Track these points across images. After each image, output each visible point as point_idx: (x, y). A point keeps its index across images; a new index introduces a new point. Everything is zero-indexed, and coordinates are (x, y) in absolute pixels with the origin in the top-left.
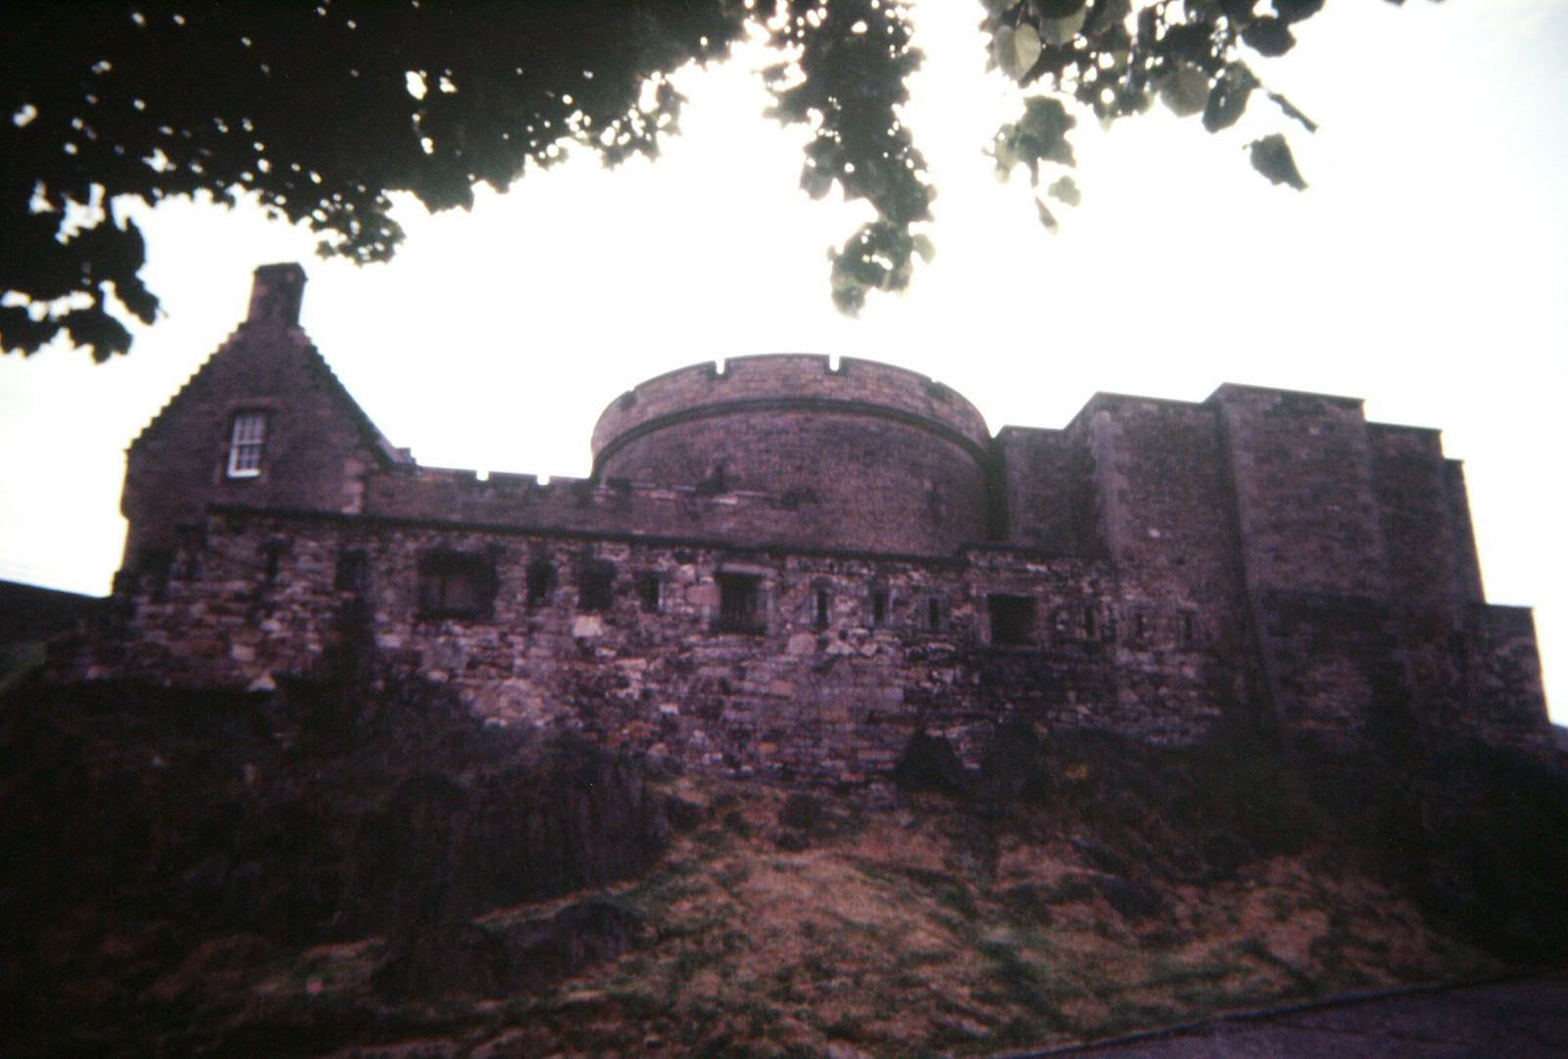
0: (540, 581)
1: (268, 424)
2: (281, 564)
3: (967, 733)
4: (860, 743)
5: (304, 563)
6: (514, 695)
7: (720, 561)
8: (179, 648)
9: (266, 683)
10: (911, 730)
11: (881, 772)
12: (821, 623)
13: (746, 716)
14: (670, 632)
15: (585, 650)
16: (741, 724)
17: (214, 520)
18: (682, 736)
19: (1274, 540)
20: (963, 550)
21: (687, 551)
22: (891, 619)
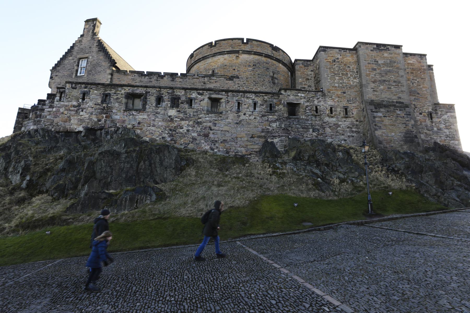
0: (159, 100)
1: (87, 61)
2: (86, 97)
3: (280, 140)
5: (92, 96)
6: (151, 131)
7: (210, 94)
8: (56, 120)
9: (81, 129)
10: (263, 140)
11: (254, 151)
12: (239, 110)
13: (216, 136)
14: (195, 114)
15: (171, 119)
17: (68, 86)
18: (197, 142)
19: (373, 85)
20: (280, 90)
21: (201, 92)
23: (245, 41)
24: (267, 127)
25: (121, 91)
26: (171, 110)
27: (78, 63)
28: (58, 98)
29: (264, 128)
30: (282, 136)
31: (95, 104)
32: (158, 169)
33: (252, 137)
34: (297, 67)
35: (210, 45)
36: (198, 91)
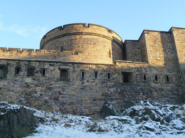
0: (18, 70)
4: (92, 105)
7: (60, 65)
10: (104, 102)
11: (96, 112)
13: (65, 99)
14: (47, 81)
15: (28, 86)
16: (63, 101)
18: (49, 104)
21: (52, 63)
22: (98, 77)
23: (87, 26)
24: (106, 92)
26: (27, 78)
29: (104, 92)
30: (118, 99)
32: (15, 127)
33: (94, 100)
34: (127, 46)
35: (60, 28)
36: (50, 63)
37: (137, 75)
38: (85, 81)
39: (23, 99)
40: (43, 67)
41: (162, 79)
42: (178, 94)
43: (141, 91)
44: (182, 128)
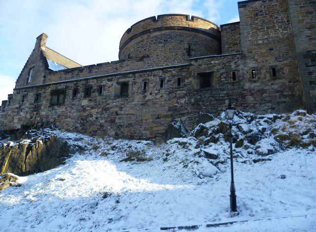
0: (75, 92)
3: (188, 118)
7: (119, 78)
8: (6, 121)
9: (19, 127)
10: (170, 119)
13: (122, 121)
15: (84, 110)
24: (174, 104)
25: (48, 90)
27: (29, 72)
28: (8, 103)
31: (30, 104)
33: (158, 118)
34: (223, 33)
35: (129, 31)
37: (222, 74)
38: (147, 94)
39: (78, 125)
40: (100, 84)
41: (266, 74)
42: (293, 96)
43: (226, 98)
44: (267, 152)
